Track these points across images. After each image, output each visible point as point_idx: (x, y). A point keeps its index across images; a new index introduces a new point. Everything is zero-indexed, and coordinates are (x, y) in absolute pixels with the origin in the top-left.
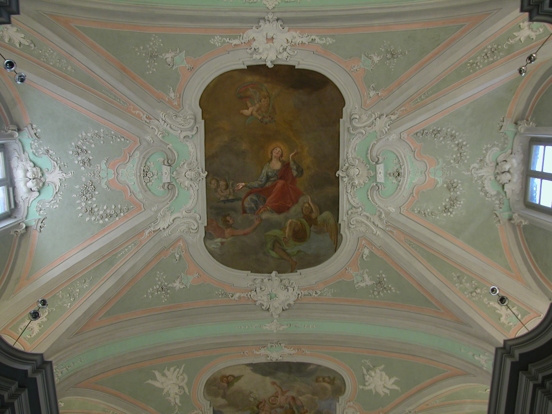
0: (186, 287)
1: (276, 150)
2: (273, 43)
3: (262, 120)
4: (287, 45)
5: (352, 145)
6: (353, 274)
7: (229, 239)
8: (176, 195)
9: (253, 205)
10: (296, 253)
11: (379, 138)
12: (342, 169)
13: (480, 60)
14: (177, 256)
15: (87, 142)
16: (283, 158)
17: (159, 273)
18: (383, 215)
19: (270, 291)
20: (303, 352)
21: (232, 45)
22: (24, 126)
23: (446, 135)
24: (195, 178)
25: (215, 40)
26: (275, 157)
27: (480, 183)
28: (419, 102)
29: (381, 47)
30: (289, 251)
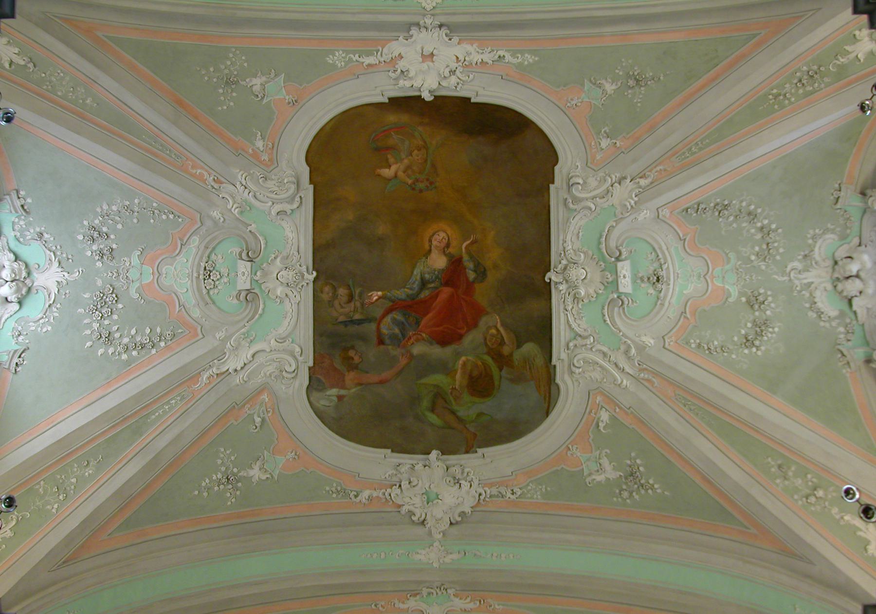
0: (272, 476)
1: (438, 235)
2: (433, 62)
3: (413, 186)
4: (456, 65)
5: (572, 228)
6: (581, 458)
7: (353, 390)
8: (260, 311)
9: (397, 331)
10: (474, 418)
11: (620, 217)
12: (556, 268)
13: (791, 90)
14: (258, 420)
15: (109, 221)
16: (451, 250)
17: (222, 450)
18: (633, 351)
19: (427, 486)
20: (490, 606)
21: (364, 65)
22: (5, 193)
23: (739, 213)
24: (295, 282)
25: (335, 57)
26: (436, 247)
27: (808, 295)
28: (688, 157)
29: (617, 68)
30: (461, 413)
